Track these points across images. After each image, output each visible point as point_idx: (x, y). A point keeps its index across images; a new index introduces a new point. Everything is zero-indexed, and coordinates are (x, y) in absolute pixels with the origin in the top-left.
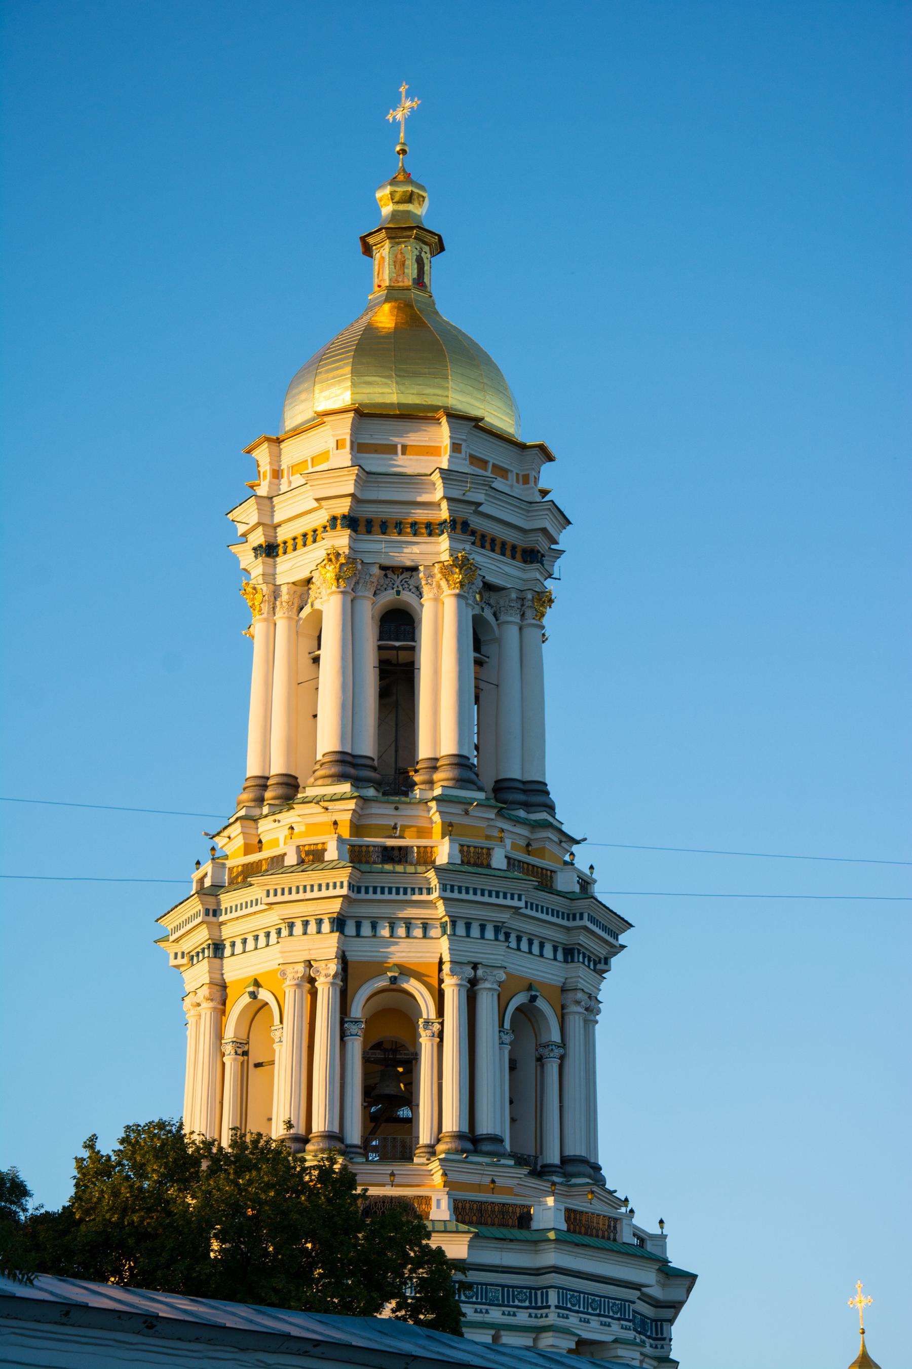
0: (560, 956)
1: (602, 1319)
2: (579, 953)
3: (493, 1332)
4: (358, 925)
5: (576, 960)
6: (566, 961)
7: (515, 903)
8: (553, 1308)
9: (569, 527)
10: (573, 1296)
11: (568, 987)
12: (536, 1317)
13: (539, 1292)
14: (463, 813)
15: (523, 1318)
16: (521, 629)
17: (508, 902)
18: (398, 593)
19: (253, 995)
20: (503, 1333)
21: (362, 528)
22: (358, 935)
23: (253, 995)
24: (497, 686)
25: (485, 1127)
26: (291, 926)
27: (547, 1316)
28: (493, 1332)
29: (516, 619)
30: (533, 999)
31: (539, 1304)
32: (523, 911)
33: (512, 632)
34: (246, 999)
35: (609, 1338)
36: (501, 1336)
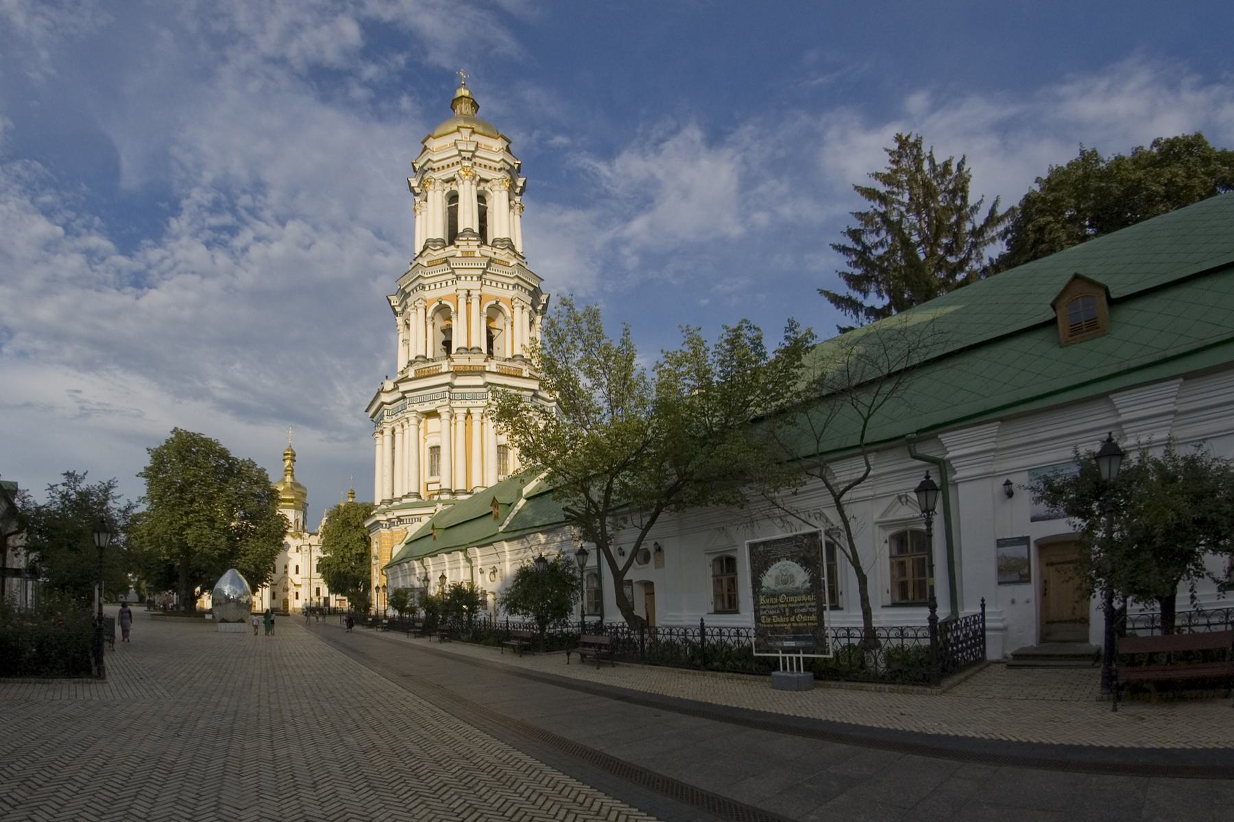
19: (440, 302)
23: (440, 302)
34: (438, 304)
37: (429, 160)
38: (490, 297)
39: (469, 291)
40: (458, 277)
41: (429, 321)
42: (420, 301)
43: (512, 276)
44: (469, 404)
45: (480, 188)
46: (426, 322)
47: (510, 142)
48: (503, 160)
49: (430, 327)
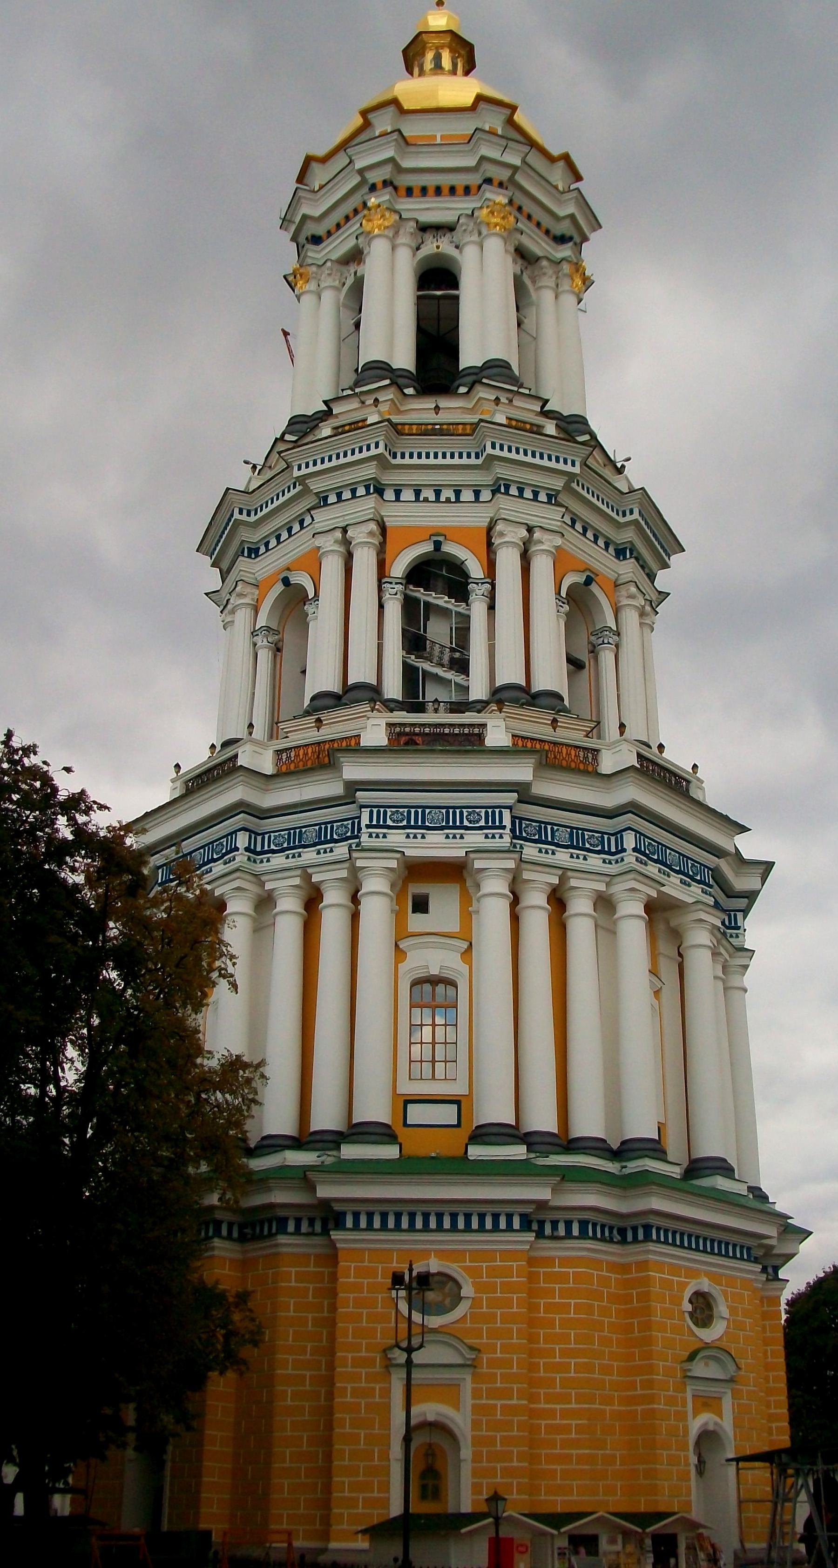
0: (611, 549)
1: (681, 876)
2: (631, 554)
3: (560, 872)
4: (398, 493)
5: (628, 556)
6: (617, 557)
7: (568, 468)
8: (629, 851)
9: (599, 231)
10: (650, 844)
11: (620, 582)
12: (610, 863)
13: (613, 839)
14: (507, 402)
15: (595, 862)
16: (556, 297)
17: (561, 466)
18: (438, 247)
19: (286, 582)
20: (570, 874)
21: (403, 192)
22: (398, 499)
23: (286, 582)
24: (535, 339)
25: (540, 684)
26: (325, 498)
27: (622, 860)
28: (560, 872)
29: (553, 285)
30: (589, 581)
31: (613, 849)
32: (574, 485)
33: (547, 296)
34: (279, 587)
35: (690, 900)
36: (569, 878)
37: (305, 218)
38: (412, 535)
39: (345, 530)
40: (323, 501)
41: (261, 641)
42: (238, 588)
43: (479, 462)
44: (309, 856)
45: (431, 246)
46: (255, 645)
47: (513, 108)
48: (483, 158)
49: (265, 656)
